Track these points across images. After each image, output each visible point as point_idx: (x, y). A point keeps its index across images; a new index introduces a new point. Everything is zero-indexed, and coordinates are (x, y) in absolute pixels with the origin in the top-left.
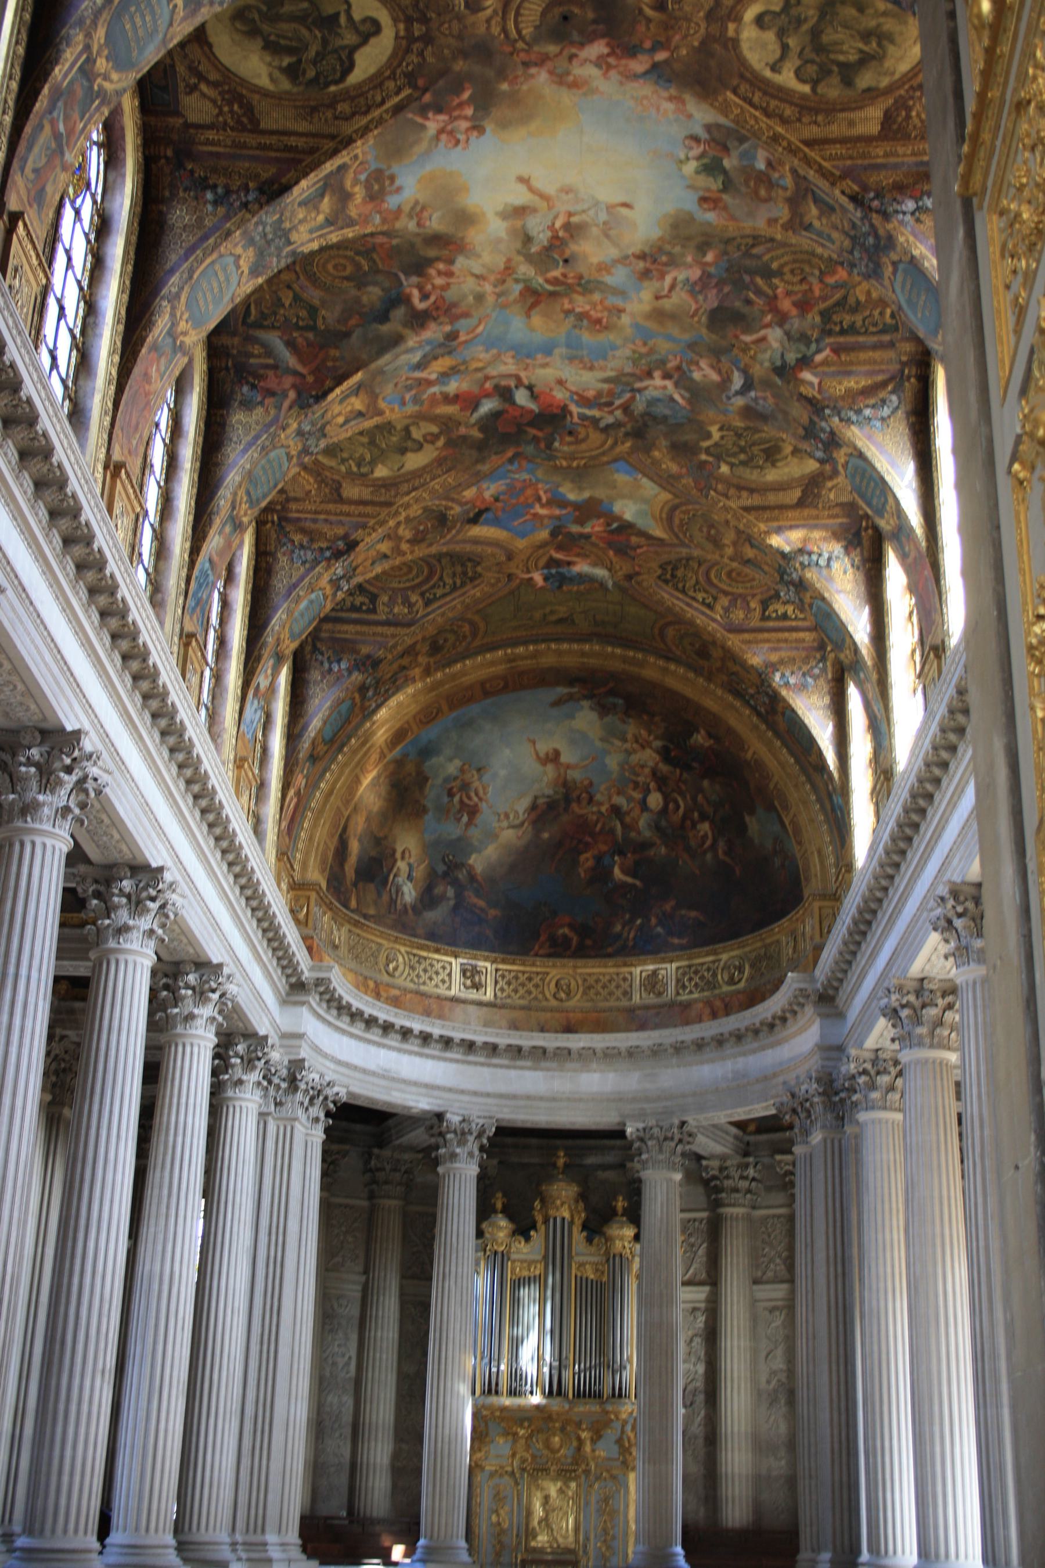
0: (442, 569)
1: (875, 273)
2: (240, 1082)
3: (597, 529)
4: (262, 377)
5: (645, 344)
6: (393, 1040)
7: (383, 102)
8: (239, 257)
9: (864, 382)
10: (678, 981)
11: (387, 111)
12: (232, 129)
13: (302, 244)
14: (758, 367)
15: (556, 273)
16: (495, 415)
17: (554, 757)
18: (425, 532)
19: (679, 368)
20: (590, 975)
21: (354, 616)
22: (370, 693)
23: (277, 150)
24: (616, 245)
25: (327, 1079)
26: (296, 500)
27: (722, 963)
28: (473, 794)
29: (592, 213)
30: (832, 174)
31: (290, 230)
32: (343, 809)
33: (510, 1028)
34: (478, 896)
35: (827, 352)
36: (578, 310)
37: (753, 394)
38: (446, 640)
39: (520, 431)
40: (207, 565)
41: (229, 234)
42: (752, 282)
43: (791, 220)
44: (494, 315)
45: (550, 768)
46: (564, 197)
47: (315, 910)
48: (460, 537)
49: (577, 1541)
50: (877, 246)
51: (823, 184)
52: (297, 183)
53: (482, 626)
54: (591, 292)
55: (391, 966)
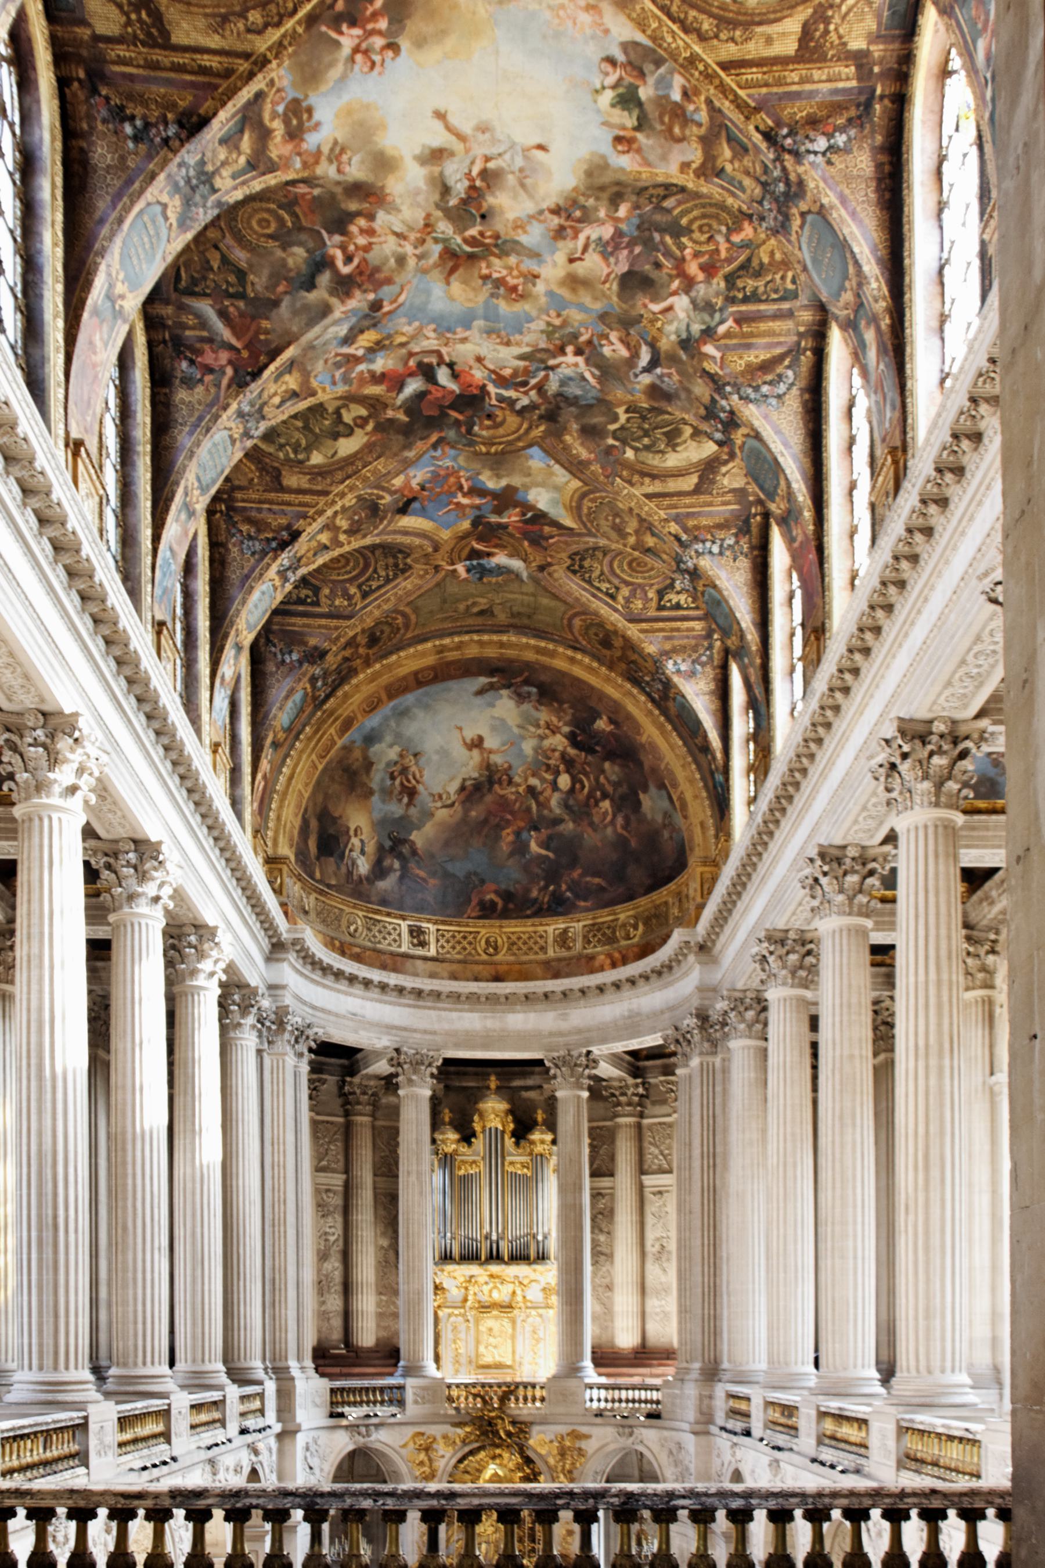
1: (782, 228)
2: (239, 1025)
4: (200, 352)
5: (559, 315)
7: (295, 11)
8: (165, 206)
9: (764, 356)
11: (299, 23)
12: (143, 44)
13: (227, 192)
14: (664, 341)
15: (473, 232)
16: (420, 396)
17: (477, 743)
18: (360, 522)
19: (590, 342)
21: (301, 608)
23: (192, 72)
24: (531, 196)
26: (240, 488)
29: (507, 157)
30: (748, 106)
31: (214, 173)
35: (730, 323)
36: (495, 275)
37: (659, 371)
39: (444, 415)
41: (153, 176)
42: (663, 242)
43: (703, 165)
44: (415, 281)
45: (476, 752)
46: (481, 137)
47: (289, 881)
50: (786, 194)
51: (737, 117)
52: (215, 114)
53: (413, 617)
54: (507, 254)
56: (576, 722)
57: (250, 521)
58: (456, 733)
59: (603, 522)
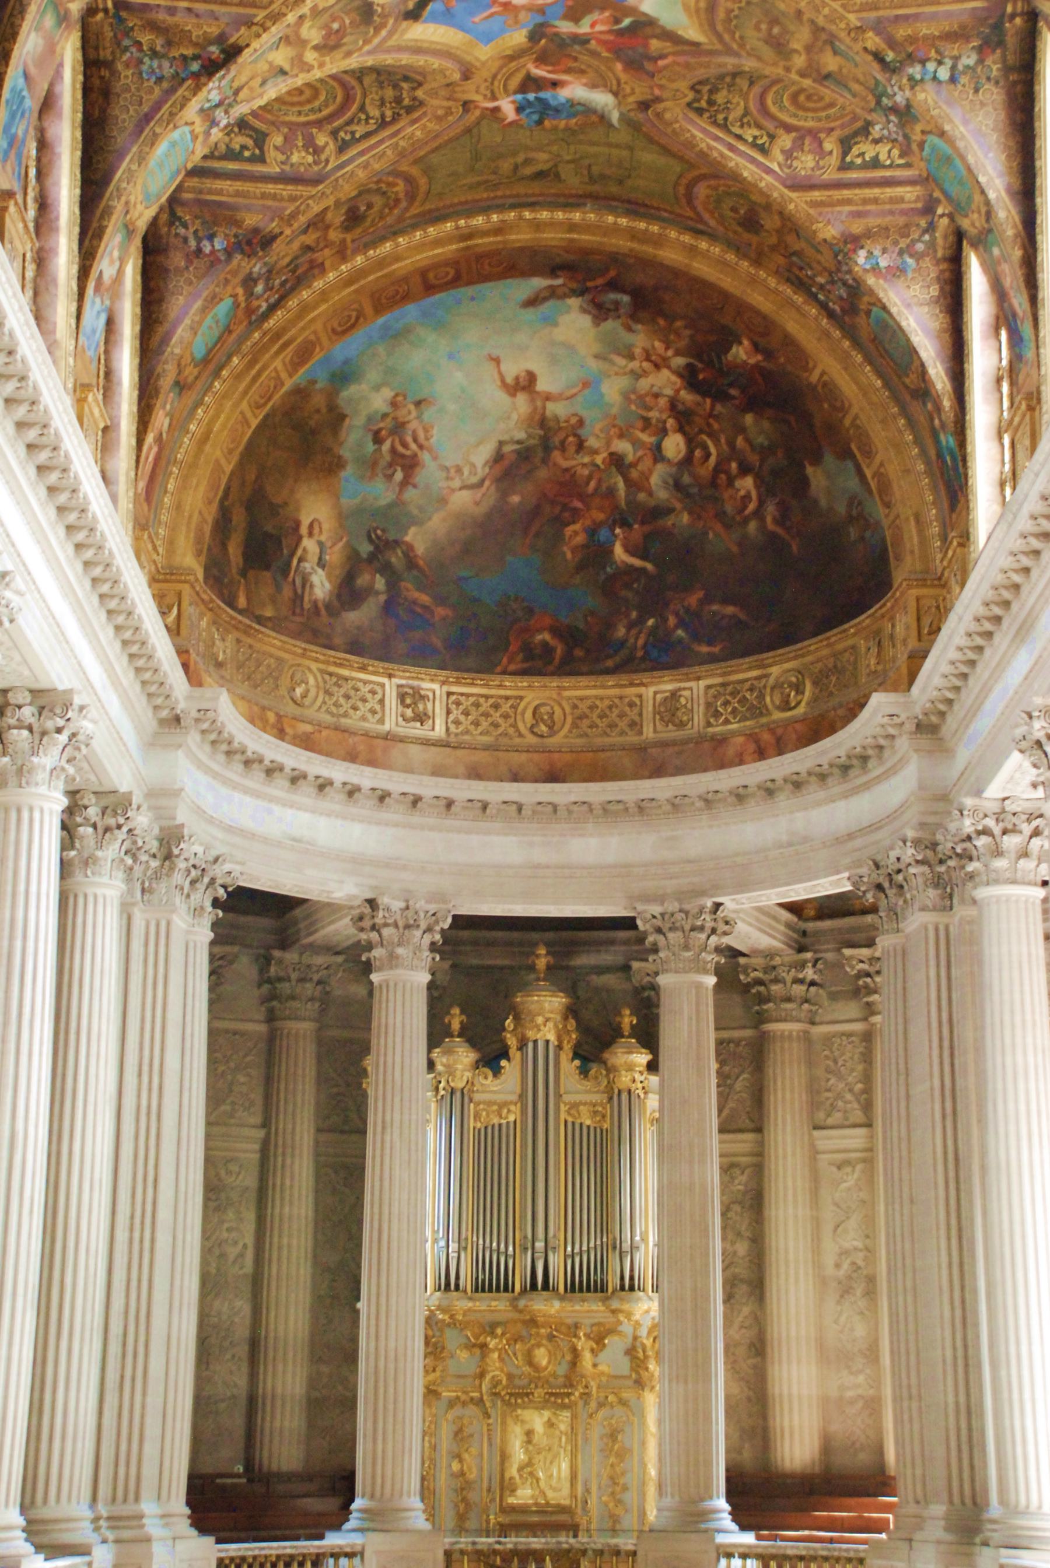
0: (365, 95)
3: (599, 28)
6: (305, 795)
10: (708, 705)
17: (526, 384)
18: (340, 33)
20: (581, 699)
21: (232, 166)
22: (259, 288)
25: (214, 853)
27: (771, 681)
28: (409, 439)
32: (223, 461)
33: (469, 777)
34: (418, 589)
38: (370, 206)
40: (21, 81)
45: (522, 398)
48: (391, 43)
49: (573, 1496)
53: (423, 181)
55: (299, 691)
56: (695, 351)
57: (153, 26)
58: (491, 367)
59: (750, 33)
